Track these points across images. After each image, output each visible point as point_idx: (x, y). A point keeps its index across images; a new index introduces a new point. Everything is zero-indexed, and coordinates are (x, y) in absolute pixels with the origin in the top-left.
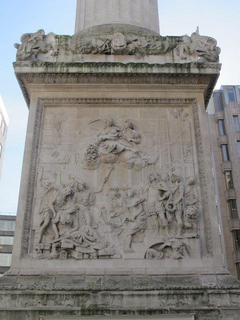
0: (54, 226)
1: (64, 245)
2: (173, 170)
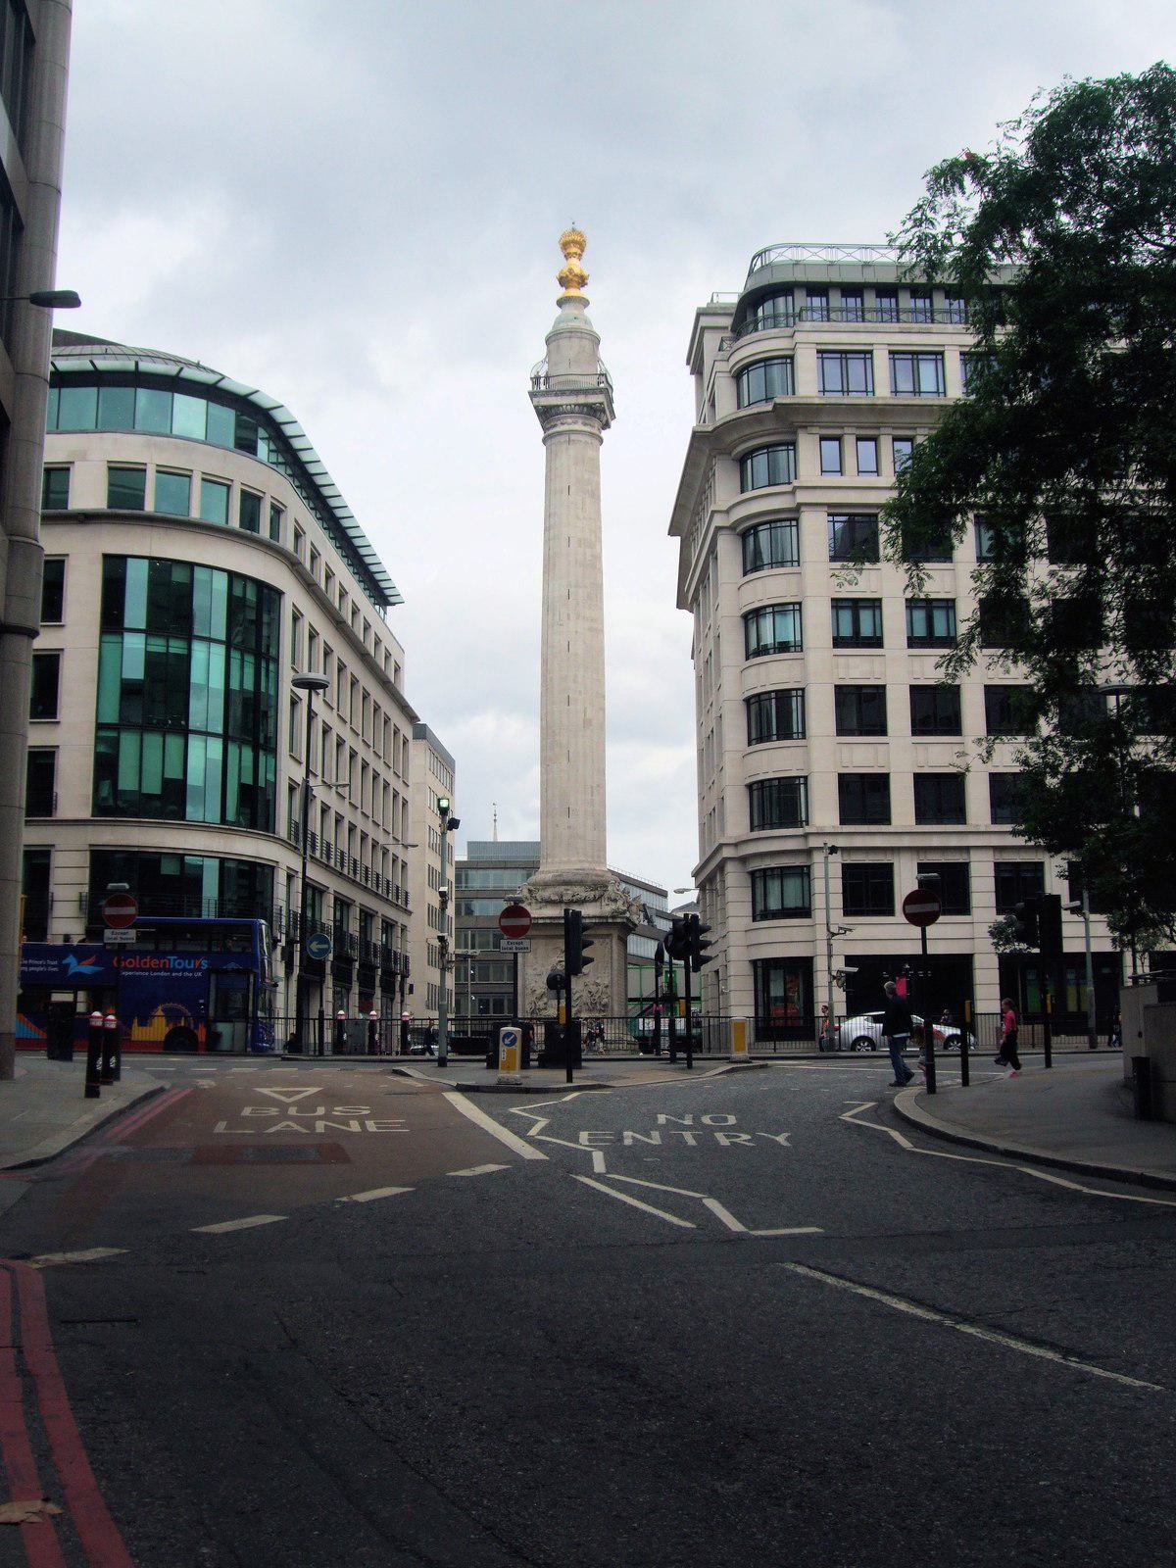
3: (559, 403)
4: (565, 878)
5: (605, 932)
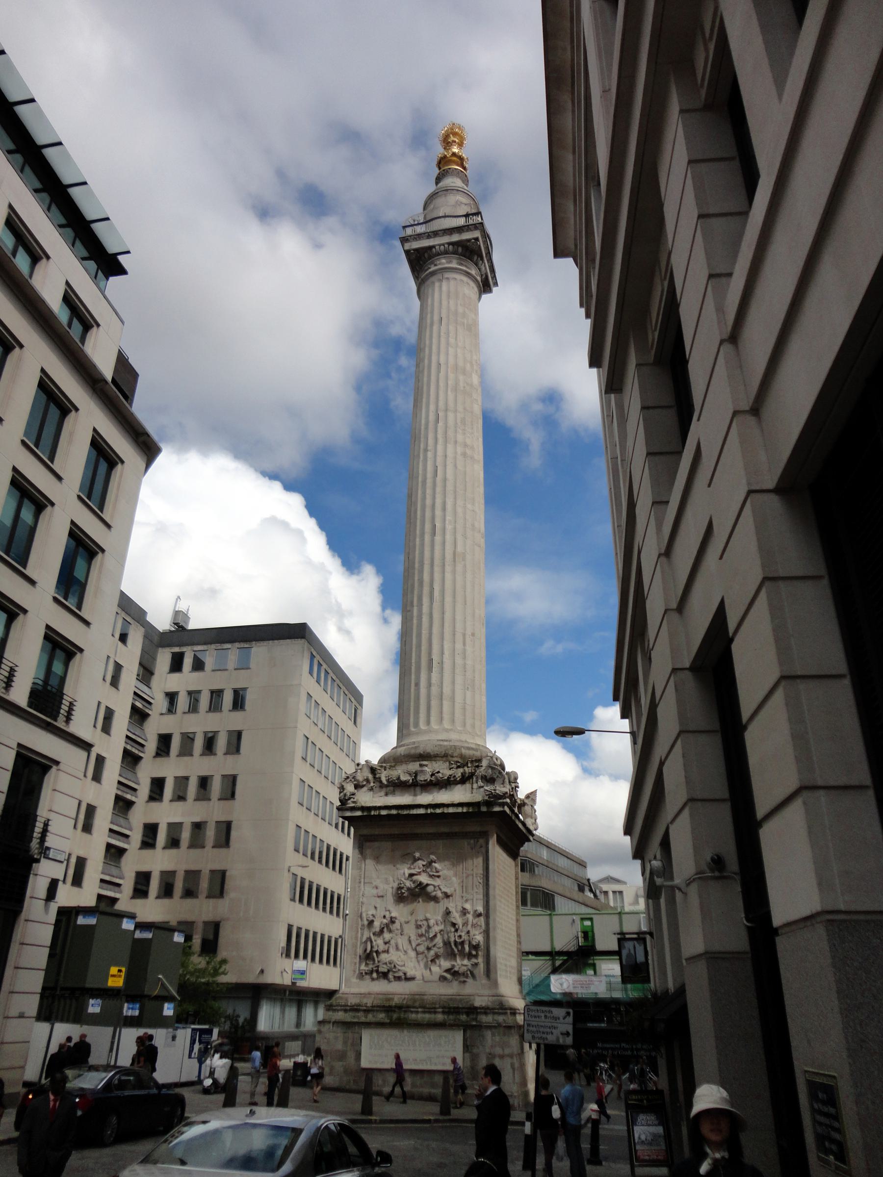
0: (375, 954)
2: (467, 901)
3: (431, 244)
4: (421, 750)
5: (477, 828)
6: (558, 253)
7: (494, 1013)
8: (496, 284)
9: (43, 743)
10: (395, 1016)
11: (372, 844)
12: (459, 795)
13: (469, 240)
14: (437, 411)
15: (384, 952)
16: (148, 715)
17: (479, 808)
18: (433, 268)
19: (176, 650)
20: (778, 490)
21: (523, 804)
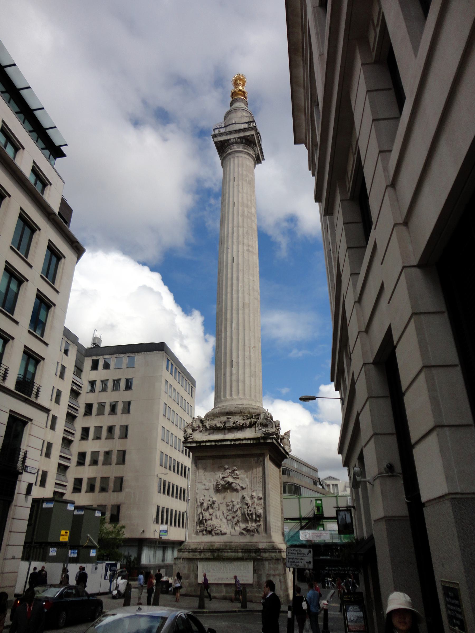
0: (204, 521)
1: (208, 529)
2: (253, 491)
3: (229, 138)
4: (227, 410)
5: (259, 452)
6: (297, 141)
7: (269, 552)
8: (263, 159)
9: (24, 409)
10: (216, 554)
11: (202, 461)
12: (248, 434)
13: (249, 136)
14: (233, 227)
15: (209, 520)
16: (80, 393)
17: (259, 441)
18: (230, 151)
19: (95, 358)
20: (419, 266)
21: (283, 438)
